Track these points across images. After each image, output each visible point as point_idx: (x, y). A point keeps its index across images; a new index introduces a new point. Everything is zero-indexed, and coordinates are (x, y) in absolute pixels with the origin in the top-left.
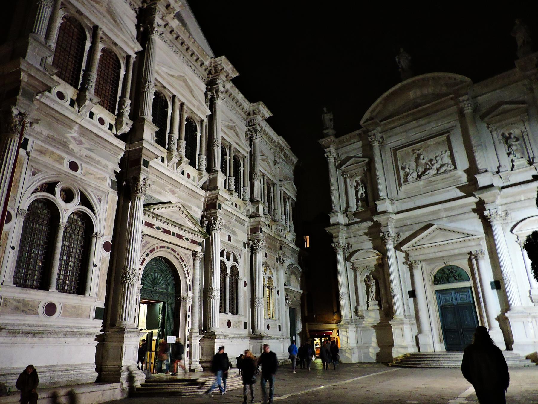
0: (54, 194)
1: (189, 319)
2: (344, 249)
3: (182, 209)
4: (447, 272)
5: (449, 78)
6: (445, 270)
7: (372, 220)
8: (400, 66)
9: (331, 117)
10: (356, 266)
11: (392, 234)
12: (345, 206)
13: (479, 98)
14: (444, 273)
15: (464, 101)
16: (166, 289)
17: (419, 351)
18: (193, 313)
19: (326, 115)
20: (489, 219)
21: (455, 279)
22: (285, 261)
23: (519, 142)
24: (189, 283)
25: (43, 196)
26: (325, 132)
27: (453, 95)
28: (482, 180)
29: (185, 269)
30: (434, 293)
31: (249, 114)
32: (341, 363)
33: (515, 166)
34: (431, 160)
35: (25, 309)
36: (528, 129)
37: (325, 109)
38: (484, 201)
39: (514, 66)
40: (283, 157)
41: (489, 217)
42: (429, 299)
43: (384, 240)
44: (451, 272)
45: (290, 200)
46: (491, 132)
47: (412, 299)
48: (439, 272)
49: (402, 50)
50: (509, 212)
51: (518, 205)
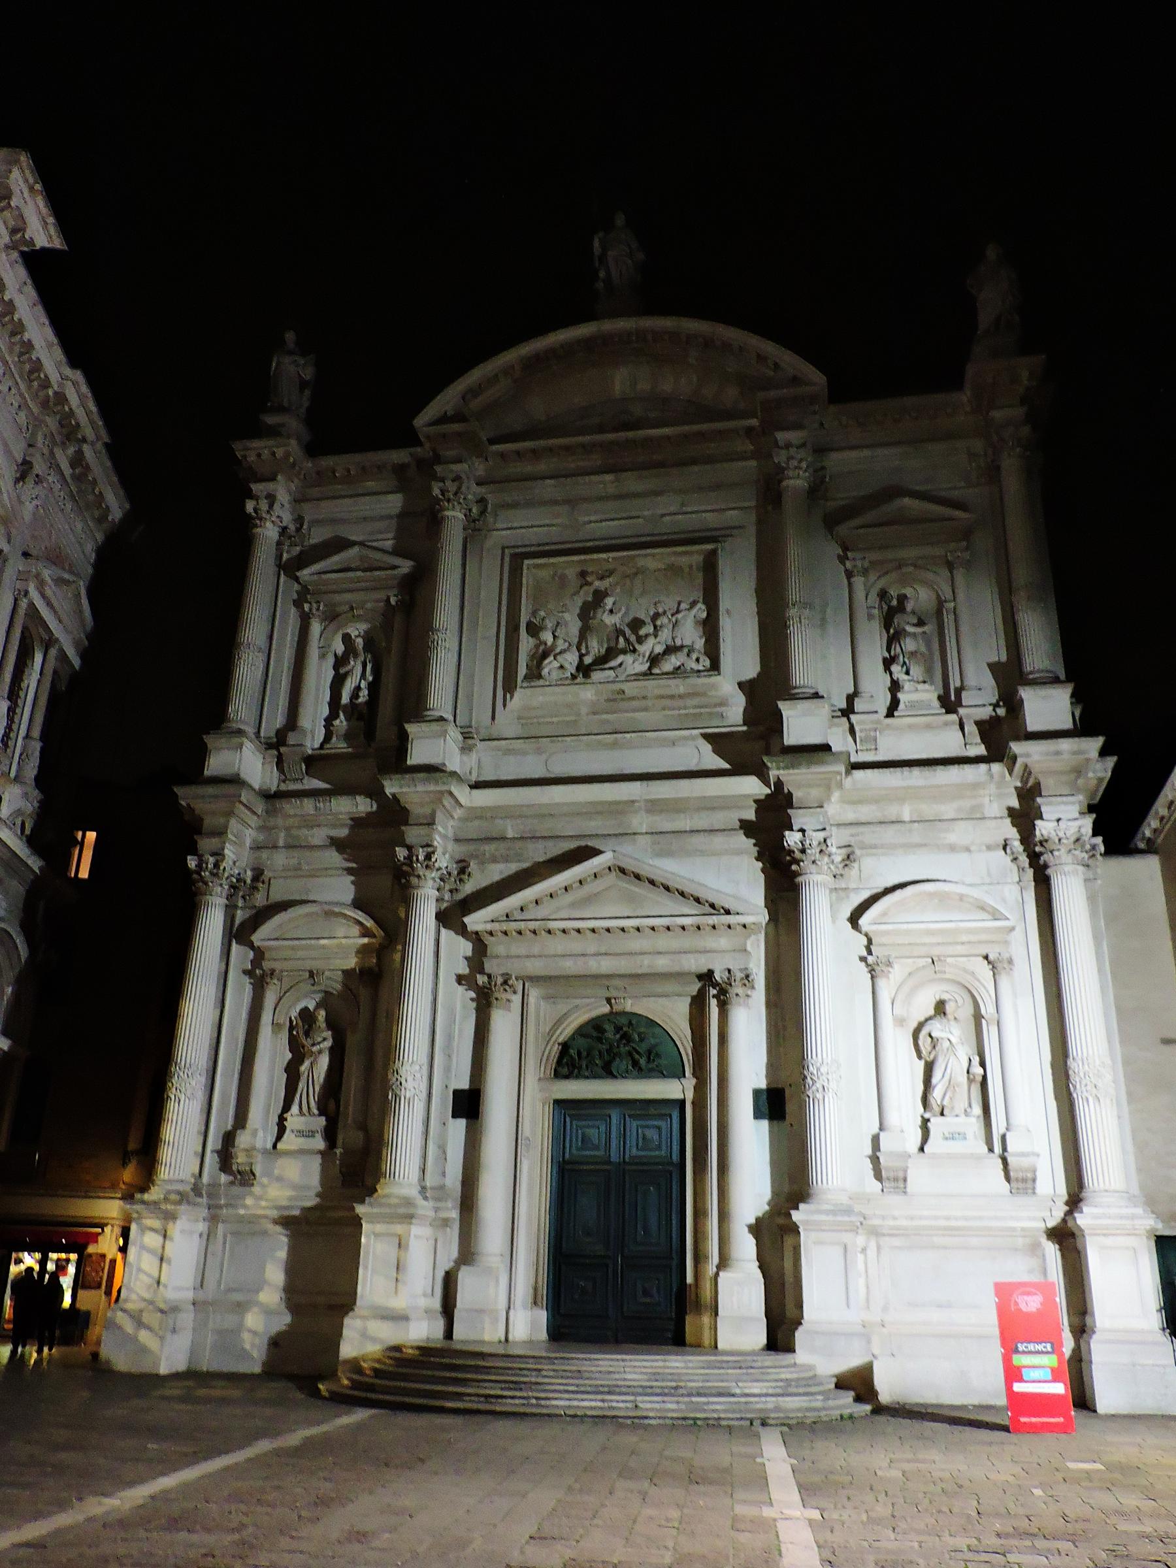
2: (232, 886)
4: (610, 1034)
5: (761, 358)
6: (608, 1027)
7: (375, 793)
8: (602, 274)
9: (308, 374)
10: (266, 965)
11: (443, 860)
12: (280, 721)
13: (834, 456)
14: (600, 1040)
15: (788, 446)
17: (449, 1334)
19: (287, 360)
20: (797, 862)
21: (635, 1064)
23: (926, 629)
26: (271, 420)
27: (754, 422)
28: (801, 724)
30: (548, 1109)
33: (901, 706)
34: (636, 624)
36: (961, 596)
37: (290, 337)
38: (790, 794)
39: (956, 383)
40: (67, 471)
41: (798, 855)
42: (526, 1129)
43: (406, 875)
44: (626, 1037)
45: (53, 652)
46: (849, 575)
47: (462, 1123)
48: (581, 1032)
49: (620, 220)
50: (858, 852)
51: (889, 834)
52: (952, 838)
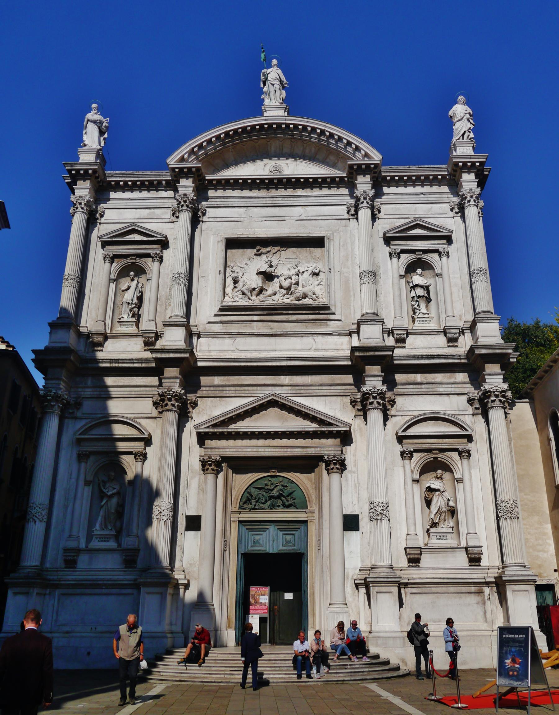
51: (411, 389)
52: (441, 390)
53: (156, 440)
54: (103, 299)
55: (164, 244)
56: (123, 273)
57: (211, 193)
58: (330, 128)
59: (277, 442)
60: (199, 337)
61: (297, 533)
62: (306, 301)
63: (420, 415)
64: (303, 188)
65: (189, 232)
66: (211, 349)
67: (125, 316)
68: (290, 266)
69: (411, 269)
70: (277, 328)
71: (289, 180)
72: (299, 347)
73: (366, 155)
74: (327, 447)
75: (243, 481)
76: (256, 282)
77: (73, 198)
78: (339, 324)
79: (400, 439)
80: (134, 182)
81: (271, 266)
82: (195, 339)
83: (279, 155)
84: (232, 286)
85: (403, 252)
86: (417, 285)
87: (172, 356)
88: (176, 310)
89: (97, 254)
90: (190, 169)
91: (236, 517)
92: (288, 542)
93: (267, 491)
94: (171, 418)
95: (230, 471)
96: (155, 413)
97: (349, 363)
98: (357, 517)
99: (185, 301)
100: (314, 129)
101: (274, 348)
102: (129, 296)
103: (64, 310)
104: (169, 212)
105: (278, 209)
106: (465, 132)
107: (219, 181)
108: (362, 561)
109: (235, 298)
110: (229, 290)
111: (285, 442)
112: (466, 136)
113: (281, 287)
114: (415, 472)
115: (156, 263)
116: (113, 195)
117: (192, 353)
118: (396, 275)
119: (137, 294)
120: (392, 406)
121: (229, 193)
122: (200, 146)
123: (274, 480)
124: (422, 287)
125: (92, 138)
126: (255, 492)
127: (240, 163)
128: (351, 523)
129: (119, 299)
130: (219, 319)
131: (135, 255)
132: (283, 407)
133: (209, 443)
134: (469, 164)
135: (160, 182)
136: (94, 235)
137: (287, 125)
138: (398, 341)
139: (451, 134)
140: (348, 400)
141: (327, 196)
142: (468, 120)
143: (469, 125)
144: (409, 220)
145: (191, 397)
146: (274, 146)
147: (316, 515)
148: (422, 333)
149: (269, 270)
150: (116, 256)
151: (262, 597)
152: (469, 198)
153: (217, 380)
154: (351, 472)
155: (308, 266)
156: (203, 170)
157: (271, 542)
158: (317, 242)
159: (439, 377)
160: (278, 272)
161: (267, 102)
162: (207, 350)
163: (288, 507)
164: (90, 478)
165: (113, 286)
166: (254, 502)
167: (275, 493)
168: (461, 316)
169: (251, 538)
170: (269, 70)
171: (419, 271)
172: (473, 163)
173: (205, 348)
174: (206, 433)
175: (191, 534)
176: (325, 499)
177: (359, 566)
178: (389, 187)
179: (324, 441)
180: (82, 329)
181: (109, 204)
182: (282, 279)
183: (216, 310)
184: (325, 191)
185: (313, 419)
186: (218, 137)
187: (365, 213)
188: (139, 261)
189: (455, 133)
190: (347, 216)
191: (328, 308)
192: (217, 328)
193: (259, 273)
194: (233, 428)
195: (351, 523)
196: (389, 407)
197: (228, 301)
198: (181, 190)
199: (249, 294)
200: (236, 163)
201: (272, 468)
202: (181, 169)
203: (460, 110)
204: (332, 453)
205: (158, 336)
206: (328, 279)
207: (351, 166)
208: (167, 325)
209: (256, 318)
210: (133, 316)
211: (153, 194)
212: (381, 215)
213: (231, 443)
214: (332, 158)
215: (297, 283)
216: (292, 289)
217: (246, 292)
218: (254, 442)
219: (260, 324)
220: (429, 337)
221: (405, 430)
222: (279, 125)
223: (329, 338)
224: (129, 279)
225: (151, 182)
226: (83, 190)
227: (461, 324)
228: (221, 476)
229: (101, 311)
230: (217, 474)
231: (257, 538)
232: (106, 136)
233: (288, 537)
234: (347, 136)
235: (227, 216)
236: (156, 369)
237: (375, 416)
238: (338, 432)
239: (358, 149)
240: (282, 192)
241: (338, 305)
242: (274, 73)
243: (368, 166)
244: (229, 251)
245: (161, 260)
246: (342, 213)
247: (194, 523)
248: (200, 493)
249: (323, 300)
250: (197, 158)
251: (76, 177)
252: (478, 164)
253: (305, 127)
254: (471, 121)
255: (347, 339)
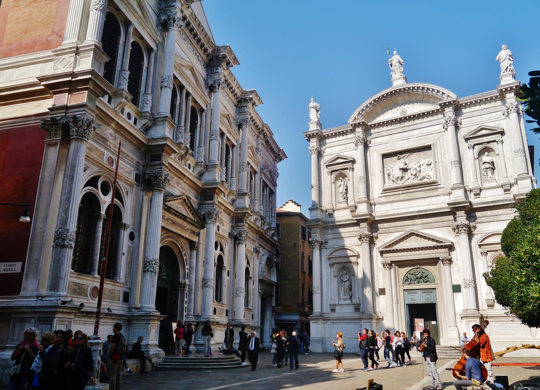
0: (97, 189)
1: (185, 305)
3: (187, 201)
16: (167, 276)
18: (190, 301)
22: (261, 251)
24: (187, 271)
25: (90, 190)
29: (185, 258)
30: (402, 292)
31: (240, 101)
32: (311, 353)
35: (80, 292)
40: (264, 144)
45: (268, 189)
51: (484, 219)
52: (501, 218)
53: (361, 255)
54: (330, 193)
55: (353, 162)
56: (337, 178)
57: (373, 131)
58: (427, 86)
59: (417, 252)
60: (375, 205)
61: (432, 294)
62: (425, 180)
63: (489, 233)
64: (418, 119)
65: (363, 155)
66: (381, 210)
67: (341, 199)
68: (415, 162)
69: (481, 153)
70: (412, 196)
71: (410, 117)
72: (424, 204)
73: (448, 96)
74: (442, 253)
75: (403, 271)
76: (399, 174)
77: (310, 148)
78: (443, 189)
79: (480, 246)
80: (336, 133)
81: (406, 164)
82: (373, 206)
83: (404, 104)
84: (388, 178)
85: (475, 145)
86: (485, 162)
87: (362, 218)
88: (362, 195)
89: (325, 171)
90: (359, 123)
91: (402, 288)
92: (427, 298)
93: (415, 275)
94: (366, 246)
95: (397, 267)
96: (359, 243)
97: (449, 210)
98: (459, 286)
99: (365, 189)
100: (418, 88)
101: (411, 206)
102: (342, 189)
103: (313, 202)
104: (354, 144)
105: (406, 133)
106: (507, 67)
107: (375, 125)
108: (464, 306)
109: (389, 184)
110: (386, 180)
111: (420, 252)
112: (508, 69)
113: (412, 175)
114: (489, 262)
115: (351, 172)
116: (328, 141)
117: (371, 215)
118: (473, 159)
119: (345, 188)
120: (475, 229)
121: (381, 129)
122: (363, 110)
123: (418, 270)
124: (488, 163)
125: (313, 116)
126: (409, 276)
127: (385, 112)
128: (457, 289)
129: (337, 191)
130: (383, 195)
131: (341, 169)
132: (418, 235)
133: (384, 255)
134: (509, 89)
135: (347, 131)
136: (322, 163)
137: (404, 89)
138: (475, 195)
139: (499, 70)
140: (450, 228)
141: (431, 121)
142: (509, 59)
143: (510, 62)
144: (478, 126)
145: (375, 234)
146: (400, 99)
147: (440, 285)
148: (489, 188)
149: (405, 167)
150: (332, 171)
151: (420, 323)
152: (511, 109)
153: (386, 225)
154: (455, 264)
155: (425, 161)
156: (366, 122)
157: (420, 299)
158: (428, 148)
159: (500, 211)
160: (410, 166)
161: (394, 75)
162: (380, 212)
163: (426, 282)
164: (336, 274)
165: (333, 186)
166: (409, 280)
167: (419, 276)
168: (512, 176)
169: (410, 297)
170: (393, 58)
171: (486, 153)
172: (511, 88)
173: (378, 210)
174: (383, 251)
175: (381, 296)
176: (443, 278)
177: (462, 309)
178: (465, 108)
179: (439, 250)
180: (323, 208)
181: (327, 146)
182: (412, 170)
183: (381, 191)
184: (430, 118)
185: (433, 240)
186: (371, 103)
187: (451, 129)
188: (343, 171)
189: (502, 68)
190: (443, 130)
191: (436, 182)
192: (383, 200)
193: (400, 169)
194: (395, 247)
195: (457, 289)
196: (473, 230)
197: (387, 186)
198: (357, 135)
199: (396, 181)
200: (383, 113)
201: (416, 264)
202: (355, 124)
203: (504, 54)
204: (444, 256)
205: (356, 207)
206: (435, 167)
207: (440, 105)
208: (359, 203)
209: (401, 192)
210: (344, 199)
211: (345, 137)
212: (462, 126)
213: (395, 254)
214: (432, 99)
215: (420, 171)
216: (417, 175)
217: (394, 180)
218: (406, 253)
219: (404, 195)
220: (494, 190)
221: (481, 242)
222: (400, 90)
223: (439, 198)
224: (340, 181)
225: (343, 132)
226: (314, 143)
227: (512, 181)
228: (392, 270)
229: (330, 199)
230: (391, 268)
231: (413, 297)
232: (319, 112)
233: (428, 296)
234: (436, 88)
235: (382, 141)
236: (357, 223)
237: (464, 237)
238: (446, 246)
239: (443, 93)
240: (408, 123)
241: (442, 179)
242: (396, 59)
243: (450, 102)
244: (384, 159)
245: (353, 169)
246: (440, 128)
247: (382, 292)
248: (383, 278)
249: (434, 179)
250: (362, 116)
251: (309, 137)
252: (514, 87)
253: (414, 88)
254: (511, 59)
255: (448, 197)
